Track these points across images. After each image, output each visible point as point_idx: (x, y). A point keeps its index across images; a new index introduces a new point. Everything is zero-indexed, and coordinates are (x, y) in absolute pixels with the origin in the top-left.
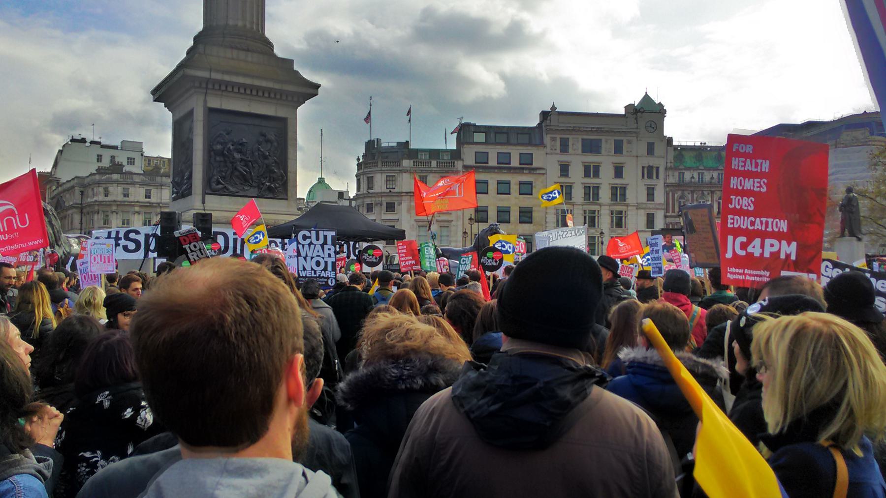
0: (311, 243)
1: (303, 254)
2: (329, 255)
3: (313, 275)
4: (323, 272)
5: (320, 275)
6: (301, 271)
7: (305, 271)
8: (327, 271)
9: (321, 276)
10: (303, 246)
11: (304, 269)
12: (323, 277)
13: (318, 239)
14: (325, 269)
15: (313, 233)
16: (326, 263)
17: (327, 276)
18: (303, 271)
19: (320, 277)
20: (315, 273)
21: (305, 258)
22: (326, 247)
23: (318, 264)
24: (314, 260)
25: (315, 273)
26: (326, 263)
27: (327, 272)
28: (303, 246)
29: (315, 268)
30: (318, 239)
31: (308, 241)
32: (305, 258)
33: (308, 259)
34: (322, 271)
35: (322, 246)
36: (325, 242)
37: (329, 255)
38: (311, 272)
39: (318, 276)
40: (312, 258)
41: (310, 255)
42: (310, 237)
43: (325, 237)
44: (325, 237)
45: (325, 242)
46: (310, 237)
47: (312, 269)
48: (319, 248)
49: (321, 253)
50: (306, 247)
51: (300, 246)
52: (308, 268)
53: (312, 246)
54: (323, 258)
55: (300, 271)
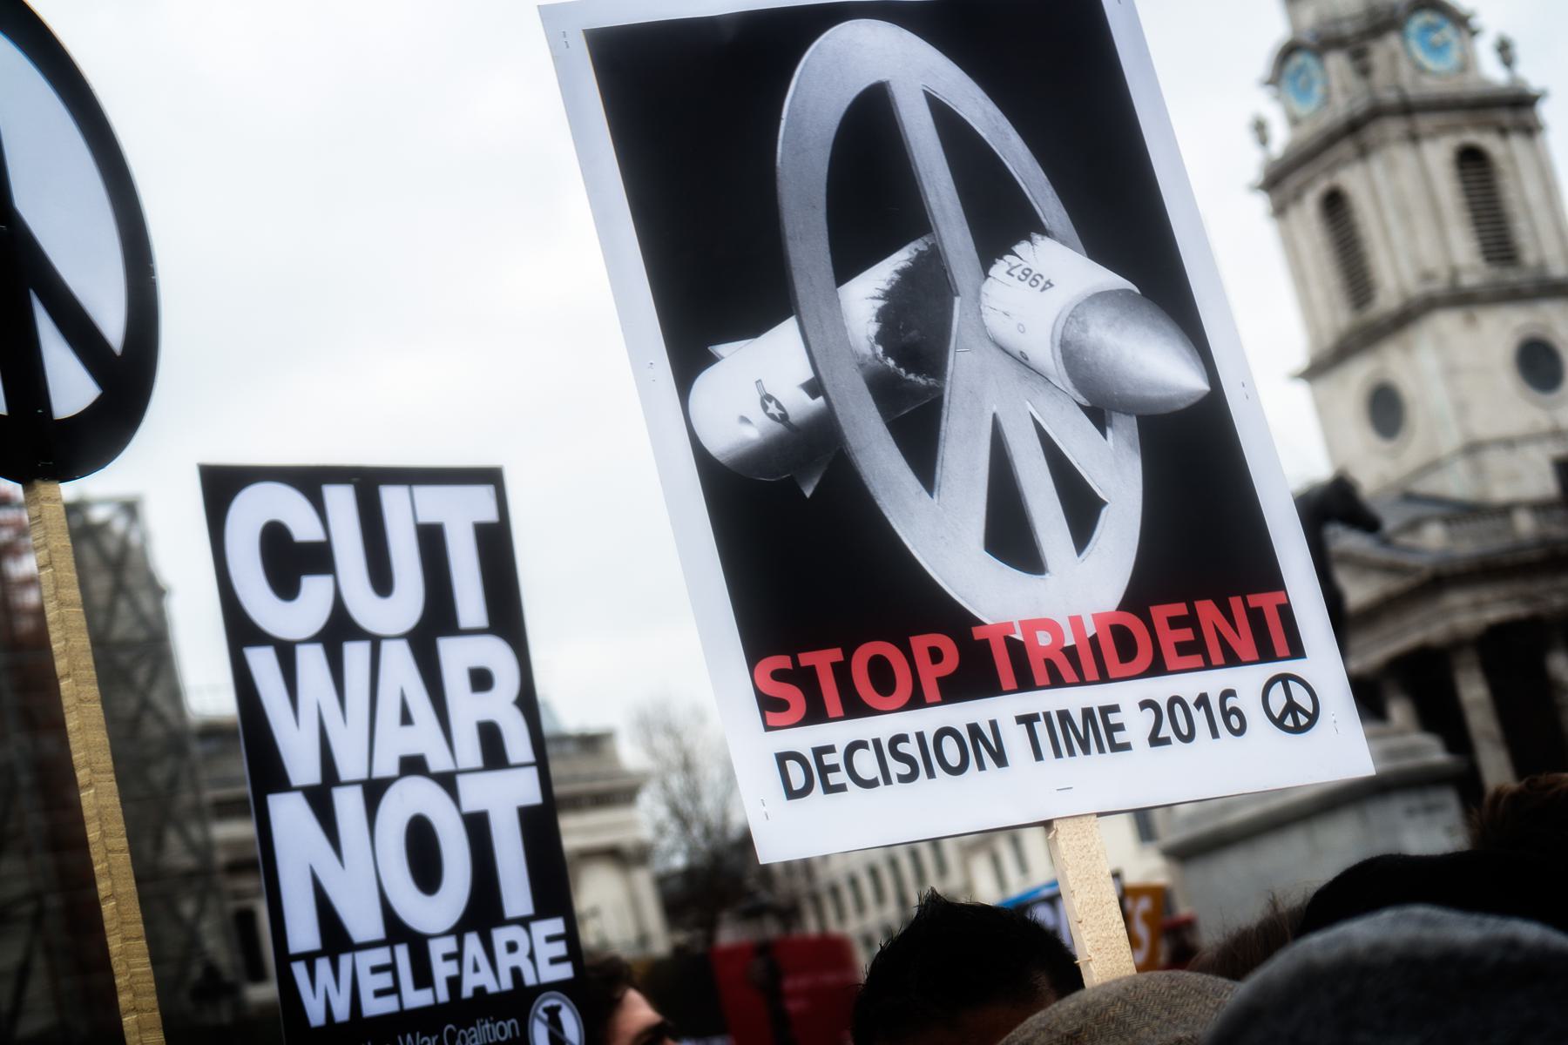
3: (416, 998)
4: (473, 943)
5: (454, 983)
6: (309, 958)
7: (345, 961)
8: (502, 922)
9: (467, 991)
10: (286, 653)
11: (335, 938)
16: (477, 827)
17: (507, 983)
18: (323, 965)
27: (501, 936)
28: (286, 653)
31: (315, 593)
34: (458, 931)
38: (392, 968)
39: (443, 995)
40: (374, 791)
47: (396, 929)
53: (356, 655)
54: (448, 782)
55: (299, 970)
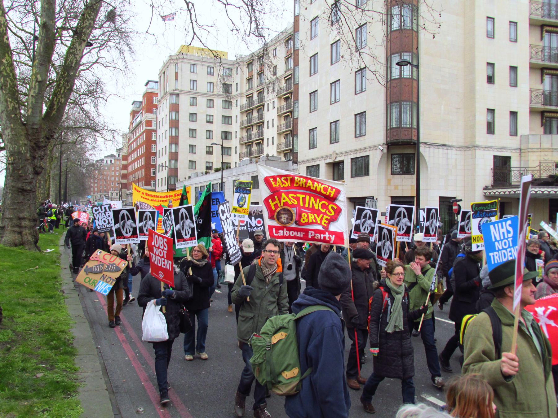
0: (99, 213)
1: (97, 218)
2: (109, 216)
11: (99, 225)
12: (109, 227)
13: (102, 210)
14: (109, 223)
15: (99, 207)
16: (108, 220)
19: (107, 228)
20: (104, 226)
21: (98, 220)
22: (107, 213)
23: (105, 221)
24: (103, 220)
25: (104, 226)
26: (108, 220)
29: (104, 224)
30: (102, 210)
31: (98, 212)
32: (98, 220)
33: (100, 220)
35: (105, 213)
36: (106, 211)
37: (109, 216)
40: (101, 219)
41: (100, 218)
42: (98, 210)
43: (105, 208)
44: (105, 208)
45: (106, 211)
46: (98, 210)
48: (103, 214)
49: (105, 216)
50: (98, 215)
51: (95, 215)
52: (101, 224)
53: (100, 214)
